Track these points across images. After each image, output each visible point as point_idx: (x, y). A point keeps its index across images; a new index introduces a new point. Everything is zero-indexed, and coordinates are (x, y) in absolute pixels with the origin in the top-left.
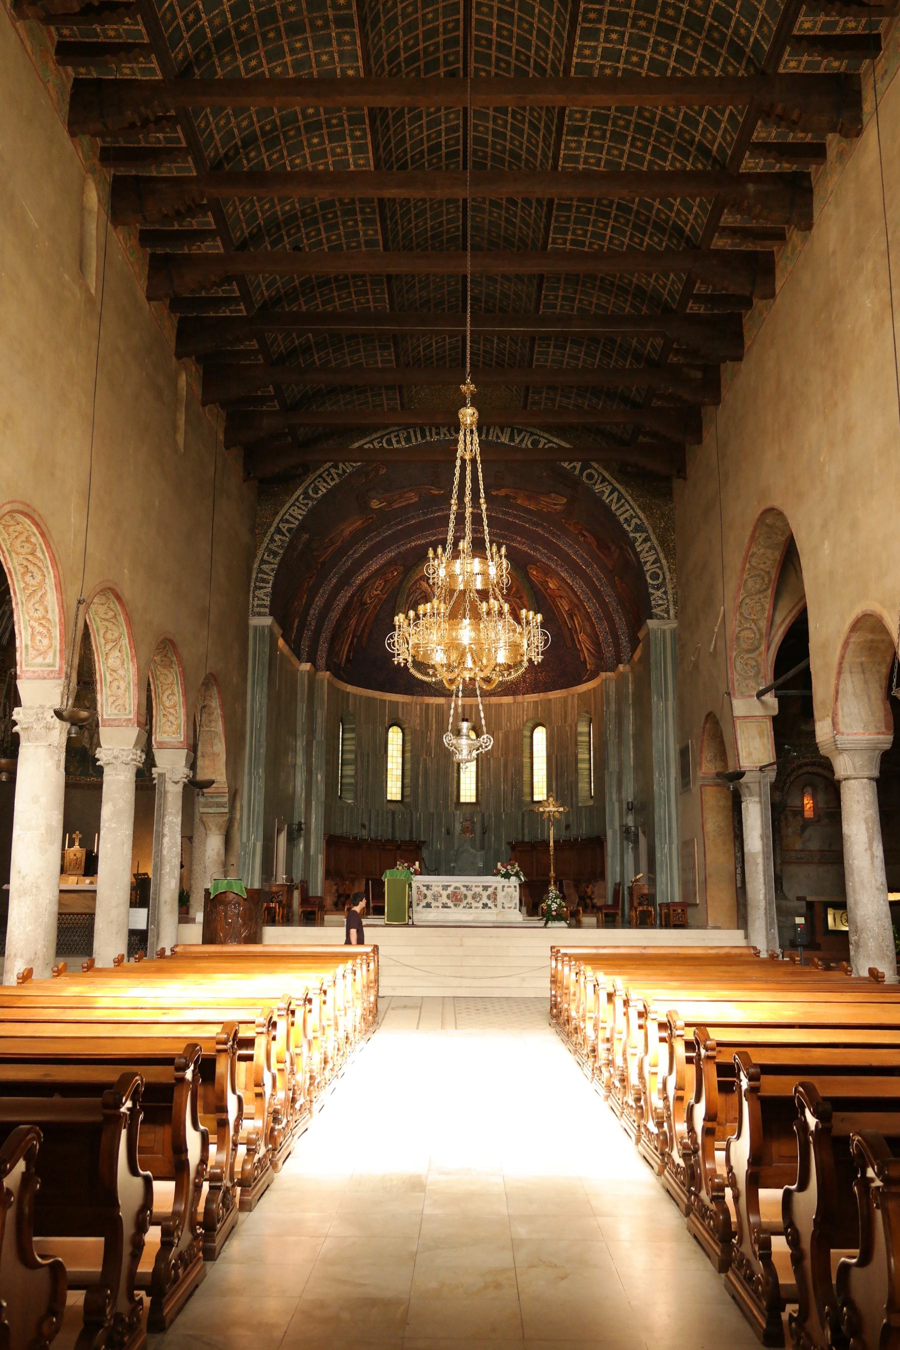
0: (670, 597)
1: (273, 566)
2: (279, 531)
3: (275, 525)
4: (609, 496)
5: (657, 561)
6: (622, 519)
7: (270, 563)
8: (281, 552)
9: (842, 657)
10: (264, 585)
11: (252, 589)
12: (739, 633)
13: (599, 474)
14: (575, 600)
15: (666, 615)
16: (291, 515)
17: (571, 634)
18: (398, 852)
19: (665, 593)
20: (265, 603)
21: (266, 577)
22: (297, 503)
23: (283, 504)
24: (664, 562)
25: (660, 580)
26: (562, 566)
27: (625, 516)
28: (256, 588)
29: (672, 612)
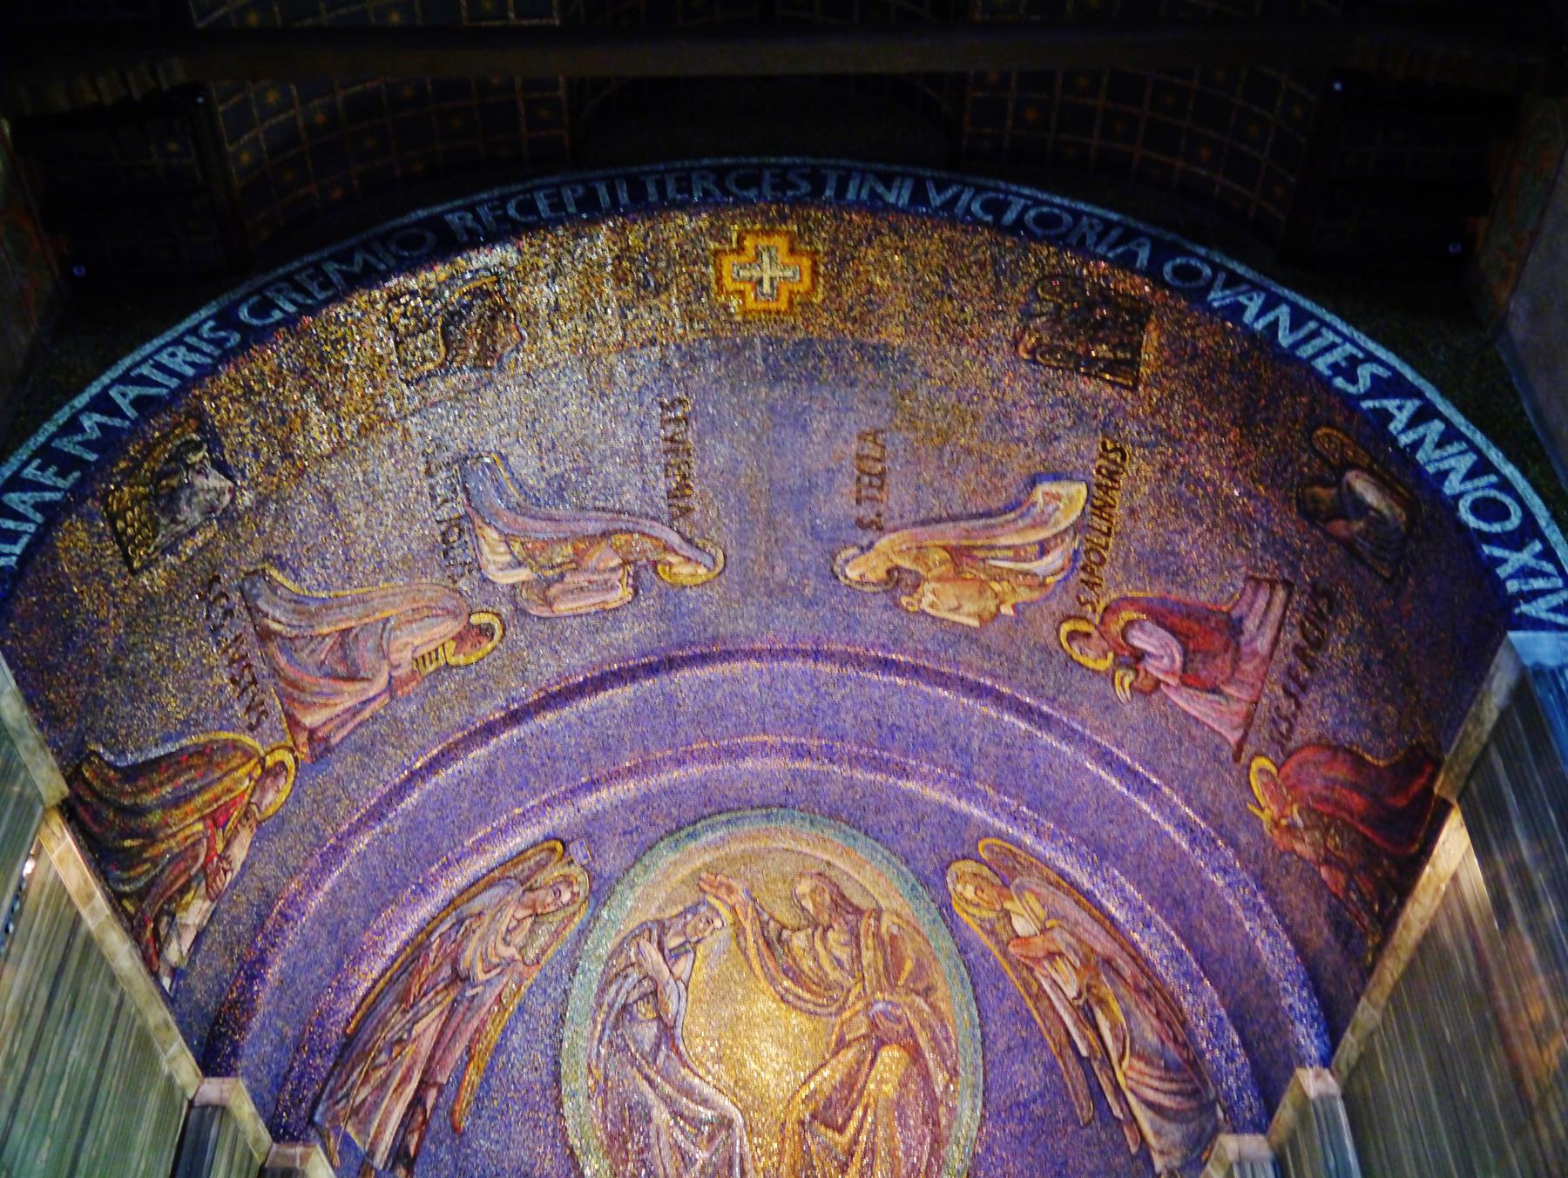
1: (48, 496)
3: (95, 389)
5: (1482, 467)
6: (1321, 364)
7: (40, 487)
8: (92, 457)
14: (1103, 944)
16: (159, 367)
17: (1089, 1074)
22: (191, 340)
23: (148, 338)
24: (1509, 470)
25: (1514, 521)
26: (1053, 837)
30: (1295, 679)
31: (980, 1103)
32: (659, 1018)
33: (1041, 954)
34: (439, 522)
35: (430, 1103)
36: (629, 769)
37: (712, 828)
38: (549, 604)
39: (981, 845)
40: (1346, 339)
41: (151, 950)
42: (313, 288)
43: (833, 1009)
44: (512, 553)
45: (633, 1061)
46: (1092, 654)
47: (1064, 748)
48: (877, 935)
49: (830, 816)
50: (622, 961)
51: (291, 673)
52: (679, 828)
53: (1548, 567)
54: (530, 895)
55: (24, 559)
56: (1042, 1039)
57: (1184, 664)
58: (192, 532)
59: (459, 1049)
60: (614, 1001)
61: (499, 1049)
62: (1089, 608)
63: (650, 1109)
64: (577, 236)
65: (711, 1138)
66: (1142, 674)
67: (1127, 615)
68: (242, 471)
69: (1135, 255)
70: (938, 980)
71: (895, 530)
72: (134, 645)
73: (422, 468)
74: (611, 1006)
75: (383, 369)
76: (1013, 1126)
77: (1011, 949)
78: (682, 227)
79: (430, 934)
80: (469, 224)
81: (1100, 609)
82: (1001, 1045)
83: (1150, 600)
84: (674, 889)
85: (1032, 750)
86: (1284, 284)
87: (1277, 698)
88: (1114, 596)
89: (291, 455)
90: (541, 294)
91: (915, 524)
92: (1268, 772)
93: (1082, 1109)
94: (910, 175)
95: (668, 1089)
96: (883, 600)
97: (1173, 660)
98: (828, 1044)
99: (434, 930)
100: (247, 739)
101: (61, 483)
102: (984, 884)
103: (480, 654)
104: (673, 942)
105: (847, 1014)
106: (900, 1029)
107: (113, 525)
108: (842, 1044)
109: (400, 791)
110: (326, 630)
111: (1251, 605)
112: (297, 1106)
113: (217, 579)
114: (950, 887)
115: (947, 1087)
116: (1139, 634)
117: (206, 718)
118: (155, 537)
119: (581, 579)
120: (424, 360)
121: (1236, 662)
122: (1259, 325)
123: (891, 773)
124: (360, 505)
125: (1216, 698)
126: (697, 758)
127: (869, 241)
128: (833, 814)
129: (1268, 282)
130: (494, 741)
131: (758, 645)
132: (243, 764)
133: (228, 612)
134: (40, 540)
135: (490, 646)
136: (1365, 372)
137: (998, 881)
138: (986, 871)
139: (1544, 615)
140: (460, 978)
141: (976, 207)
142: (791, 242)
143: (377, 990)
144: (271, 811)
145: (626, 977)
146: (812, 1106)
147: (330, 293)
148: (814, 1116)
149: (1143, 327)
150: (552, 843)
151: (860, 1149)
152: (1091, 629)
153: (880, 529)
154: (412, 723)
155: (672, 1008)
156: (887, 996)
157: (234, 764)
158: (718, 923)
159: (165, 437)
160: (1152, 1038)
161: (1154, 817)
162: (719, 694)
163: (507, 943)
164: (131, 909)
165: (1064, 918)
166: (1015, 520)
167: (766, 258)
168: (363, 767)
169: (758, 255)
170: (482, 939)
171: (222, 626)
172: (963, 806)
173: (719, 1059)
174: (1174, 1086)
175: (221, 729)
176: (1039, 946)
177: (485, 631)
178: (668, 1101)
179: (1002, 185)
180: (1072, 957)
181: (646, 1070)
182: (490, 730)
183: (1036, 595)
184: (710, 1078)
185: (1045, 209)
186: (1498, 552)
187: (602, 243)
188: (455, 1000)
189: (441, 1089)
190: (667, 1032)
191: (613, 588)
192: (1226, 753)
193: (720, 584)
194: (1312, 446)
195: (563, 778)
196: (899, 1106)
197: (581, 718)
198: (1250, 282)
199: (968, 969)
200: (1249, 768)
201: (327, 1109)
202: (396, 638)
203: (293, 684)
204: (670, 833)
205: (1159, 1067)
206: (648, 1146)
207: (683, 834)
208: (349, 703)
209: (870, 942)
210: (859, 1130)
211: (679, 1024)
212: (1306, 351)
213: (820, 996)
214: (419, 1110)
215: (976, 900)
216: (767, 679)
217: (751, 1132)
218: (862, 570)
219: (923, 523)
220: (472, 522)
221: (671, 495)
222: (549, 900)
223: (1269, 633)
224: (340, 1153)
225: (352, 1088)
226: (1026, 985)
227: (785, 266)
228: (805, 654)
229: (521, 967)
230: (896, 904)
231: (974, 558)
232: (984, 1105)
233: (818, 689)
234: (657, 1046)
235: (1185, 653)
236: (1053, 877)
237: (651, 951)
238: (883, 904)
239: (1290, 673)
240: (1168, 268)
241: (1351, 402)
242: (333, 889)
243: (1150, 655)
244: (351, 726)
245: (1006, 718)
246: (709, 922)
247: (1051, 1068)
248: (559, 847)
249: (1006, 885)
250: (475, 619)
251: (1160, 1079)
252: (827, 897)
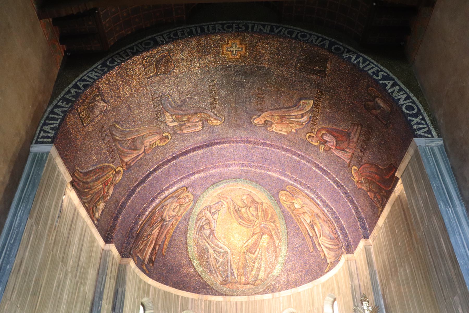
0: (429, 122)
1: (64, 109)
2: (76, 86)
3: (73, 83)
5: (408, 98)
6: (370, 72)
7: (62, 107)
8: (74, 99)
10: (53, 122)
11: (41, 125)
13: (344, 48)
14: (316, 211)
15: (429, 136)
16: (89, 77)
17: (312, 240)
19: (423, 119)
20: (49, 135)
21: (56, 116)
24: (414, 98)
25: (415, 111)
27: (373, 70)
28: (45, 124)
29: (434, 133)
30: (363, 148)
31: (286, 247)
32: (210, 228)
33: (301, 213)
34: (155, 112)
35: (157, 249)
36: (202, 170)
37: (222, 183)
38: (182, 130)
39: (287, 187)
40: (376, 66)
41: (92, 215)
42: (124, 56)
43: (252, 226)
44: (173, 118)
46: (314, 141)
47: (307, 164)
48: (262, 209)
49: (251, 181)
50: (201, 216)
51: (121, 149)
52: (214, 184)
53: (423, 122)
54: (179, 200)
55: (59, 125)
56: (301, 233)
57: (336, 144)
58: (97, 116)
59: (163, 236)
60: (200, 224)
61: (173, 236)
62: (314, 130)
63: (208, 249)
64: (188, 41)
65: (223, 256)
66: (326, 146)
67: (323, 132)
68: (108, 101)
69: (325, 45)
70: (276, 219)
71: (266, 111)
72: (85, 144)
73: (151, 99)
74: (199, 226)
75: (141, 75)
76: (294, 253)
77: (294, 212)
78: (213, 38)
79: (155, 210)
80: (162, 39)
81: (316, 130)
82: (292, 234)
83: (328, 128)
84: (213, 198)
85: (299, 164)
86: (361, 52)
87: (359, 152)
88: (320, 127)
89: (120, 97)
90: (180, 56)
91: (271, 110)
92: (356, 170)
93: (311, 248)
94: (269, 25)
95: (213, 245)
96: (263, 128)
97: (334, 143)
98: (251, 234)
99: (157, 209)
100: (112, 165)
101: (67, 106)
102: (288, 196)
103: (166, 143)
104: (213, 211)
105: (255, 227)
106: (268, 230)
107: (79, 116)
108: (254, 234)
109: (148, 176)
110: (129, 138)
111: (353, 130)
112: (127, 250)
113: (103, 127)
114: (280, 197)
115: (279, 244)
116: (326, 137)
117: (102, 160)
118: (89, 118)
119: (190, 124)
120: (151, 73)
121: (349, 143)
122: (355, 62)
123: (266, 170)
124: (136, 108)
125: (344, 152)
126: (219, 167)
127: (260, 41)
128: (251, 180)
129: (357, 52)
130: (169, 164)
131: (233, 140)
132: (111, 171)
133: (106, 135)
134: (63, 120)
135: (168, 141)
136: (380, 74)
137: (291, 195)
138: (288, 193)
139: (422, 134)
140: (163, 220)
141: (286, 33)
142: (240, 42)
143: (144, 223)
144: (118, 182)
145: (202, 219)
146: (247, 249)
147: (128, 57)
148: (247, 251)
149: (327, 62)
150: (184, 188)
151: (258, 258)
152: (314, 135)
153: (263, 111)
154: (150, 160)
155: (213, 226)
156: (265, 223)
157: (109, 171)
158: (224, 206)
159: (90, 94)
160: (327, 232)
161: (329, 180)
162: (223, 152)
163: (174, 211)
164: (87, 206)
165: (307, 204)
166: (295, 109)
167: (234, 46)
168: (139, 171)
169: (232, 45)
170: (168, 211)
171: (105, 138)
172: (283, 178)
173: (225, 238)
174: (332, 243)
175: (105, 163)
176: (301, 211)
177: (167, 137)
178: (213, 248)
179: (292, 27)
180: (309, 213)
181: (207, 241)
182: (168, 161)
183: (301, 127)
184: (222, 242)
185: (303, 33)
186: (411, 118)
187: (194, 43)
188: (162, 225)
189: (159, 245)
190: (212, 232)
191: (198, 126)
192: (346, 165)
193: (224, 125)
194: (368, 92)
195: (186, 172)
196: (267, 249)
197: (190, 158)
198: (353, 52)
199: (284, 216)
200: (351, 169)
201: (134, 251)
202: (146, 140)
203: (122, 151)
204: (212, 185)
205: (329, 239)
206: (208, 258)
207: (215, 185)
208: (135, 156)
209: (260, 210)
210: (258, 254)
211: (215, 229)
212: (366, 69)
213: (249, 223)
214: (155, 250)
215: (286, 200)
216: (235, 148)
217: (232, 255)
218: (258, 121)
219: (273, 110)
220: (163, 111)
221: (211, 103)
222: (183, 201)
223: (357, 137)
224: (137, 260)
225: (139, 245)
226: (298, 220)
227: (239, 48)
228: (244, 142)
229: (177, 217)
230: (266, 201)
231: (285, 118)
232: (288, 248)
233: (247, 150)
234: (210, 235)
235: (337, 141)
236: (305, 195)
237: (208, 213)
238: (264, 201)
239: (362, 146)
240: (333, 48)
241: (377, 81)
242: (132, 200)
243: (328, 142)
244: (135, 161)
245: (293, 157)
246: (222, 206)
247: (303, 239)
248: (186, 189)
249: (293, 197)
250: (164, 135)
251: (329, 241)
252: (250, 200)
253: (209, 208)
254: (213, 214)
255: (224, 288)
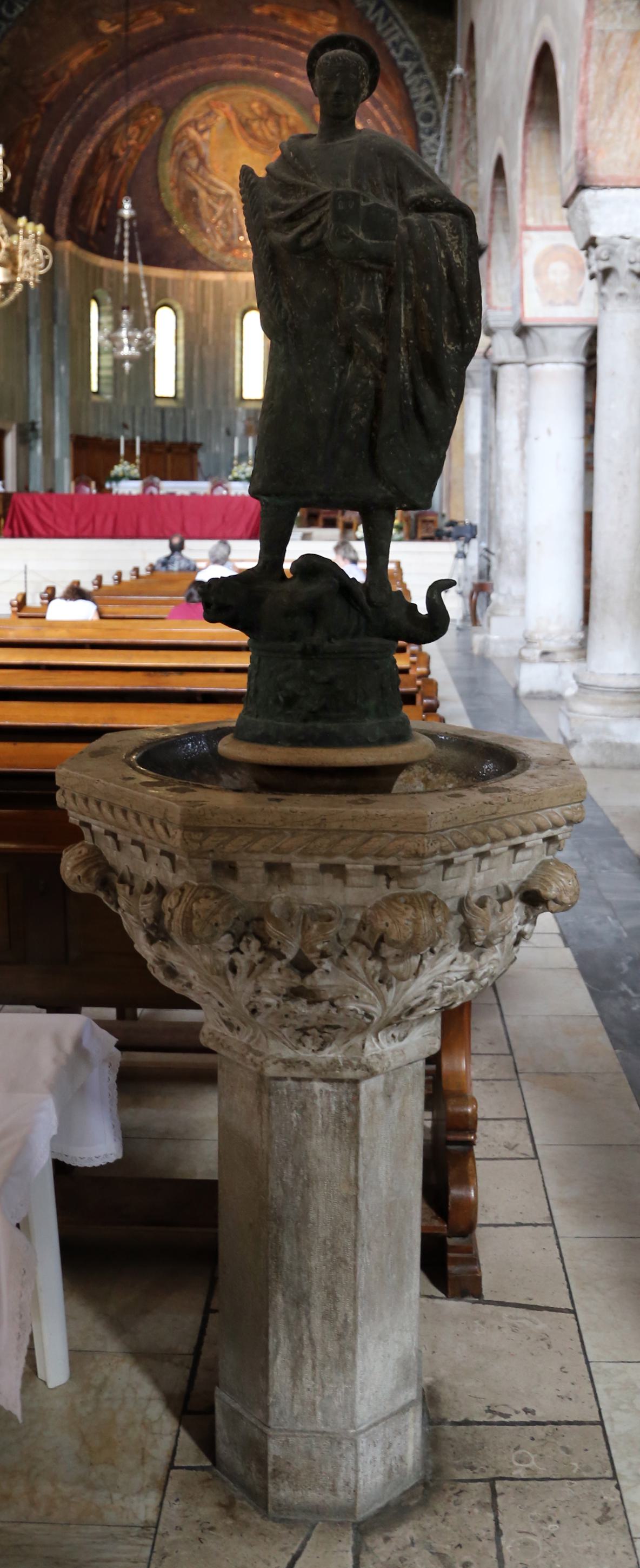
4: (374, 11)
5: (429, 98)
6: (389, 43)
9: (492, 211)
12: (465, 186)
18: (169, 457)
27: (395, 38)
40: (402, 28)
45: (190, 174)
95: (205, 184)
104: (201, 127)
140: (114, 157)
177: (106, 45)
182: (112, 73)
190: (202, 161)
212: (385, 34)
237: (192, 133)
253: (194, 123)
254: (201, 132)
255: (228, 258)
